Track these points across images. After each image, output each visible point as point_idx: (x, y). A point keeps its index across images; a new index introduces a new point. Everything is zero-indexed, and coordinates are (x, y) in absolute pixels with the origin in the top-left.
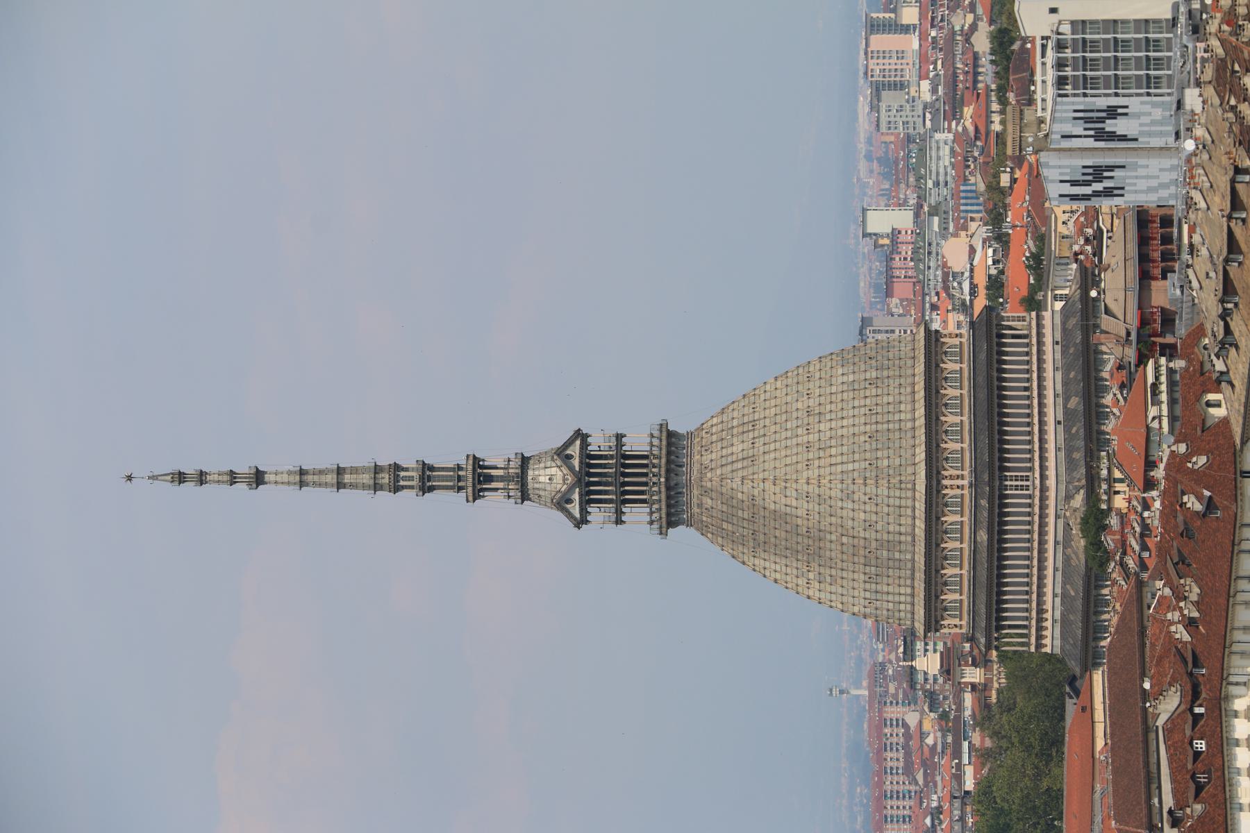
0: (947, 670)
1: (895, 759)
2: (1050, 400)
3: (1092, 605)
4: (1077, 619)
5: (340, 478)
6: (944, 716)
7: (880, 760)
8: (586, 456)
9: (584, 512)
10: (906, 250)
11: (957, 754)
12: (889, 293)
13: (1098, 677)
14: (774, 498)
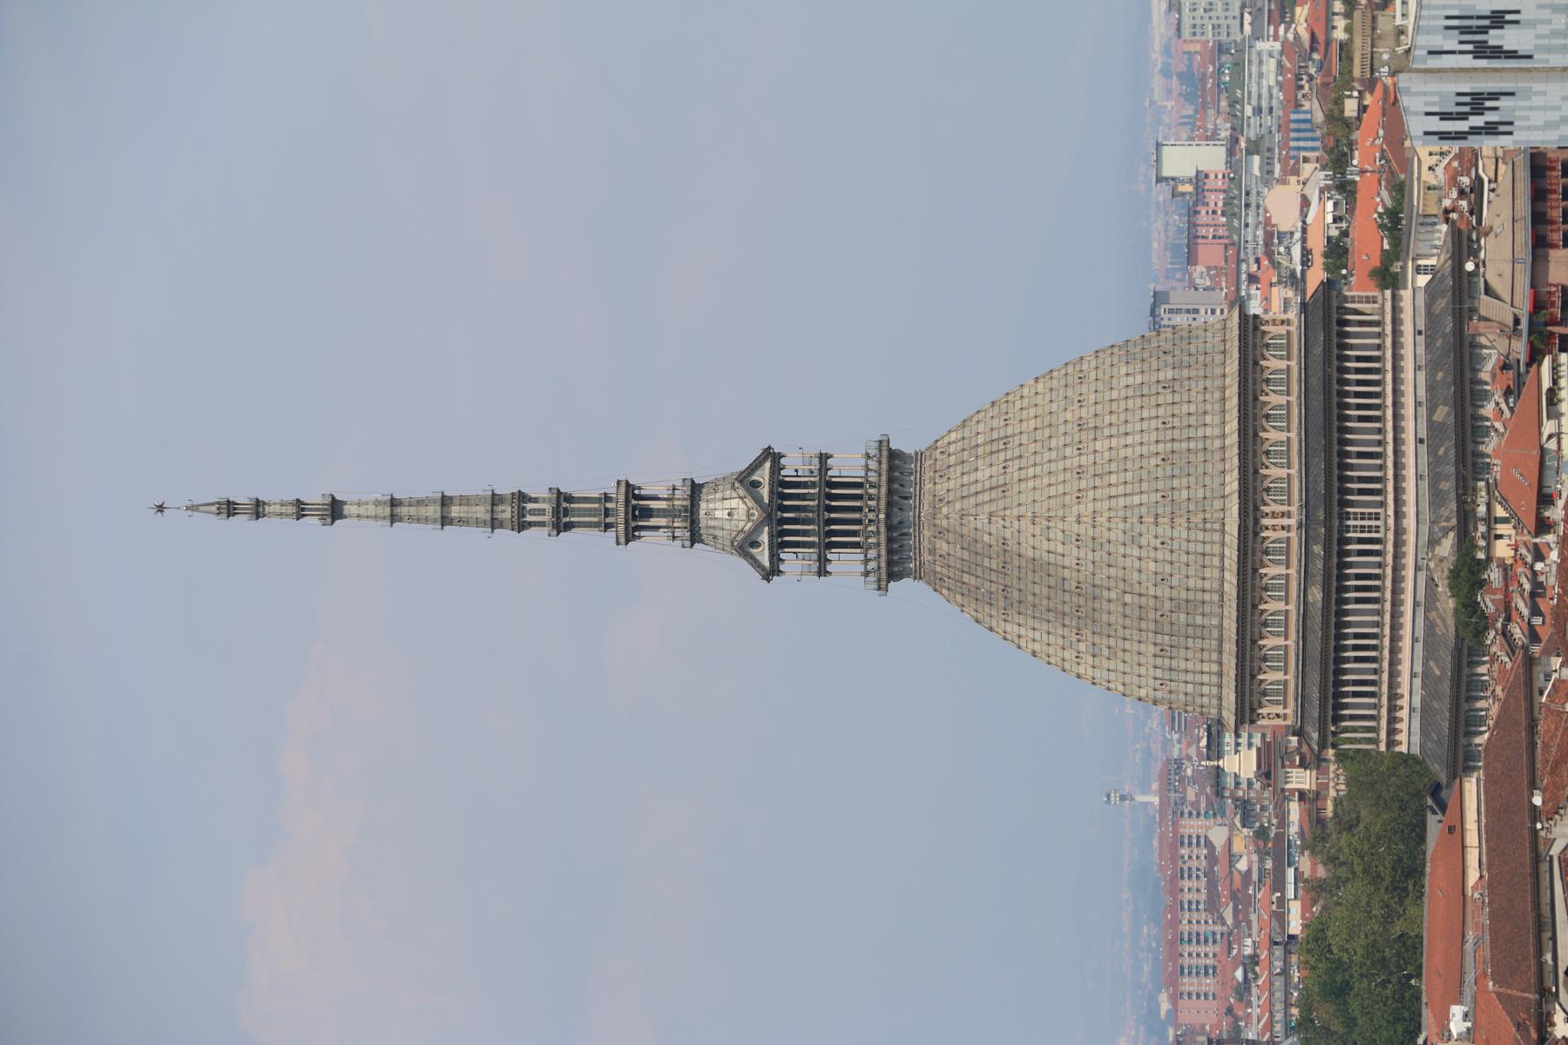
0: (1266, 773)
1: (1193, 890)
2: (1408, 411)
3: (1464, 687)
4: (1443, 707)
5: (446, 510)
6: (1261, 834)
7: (1175, 891)
8: (779, 483)
9: (775, 559)
10: (1216, 200)
11: (1279, 885)
12: (1192, 259)
13: (1471, 788)
14: (1033, 542)
